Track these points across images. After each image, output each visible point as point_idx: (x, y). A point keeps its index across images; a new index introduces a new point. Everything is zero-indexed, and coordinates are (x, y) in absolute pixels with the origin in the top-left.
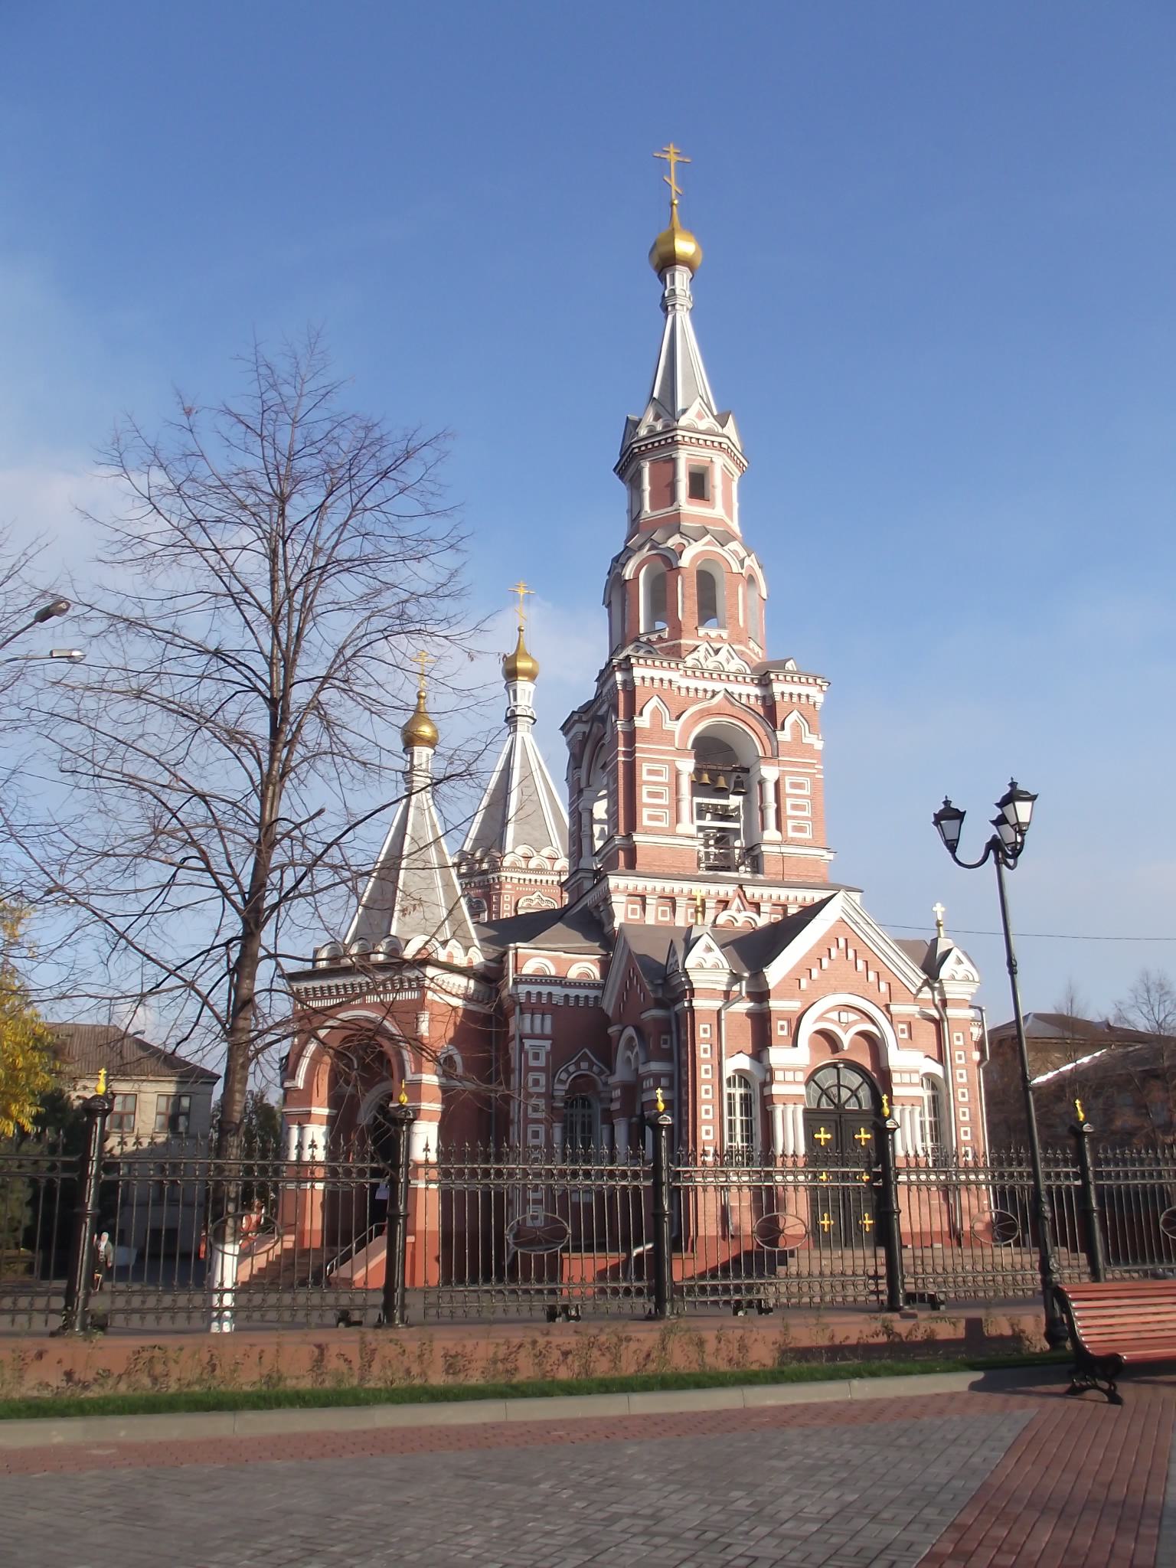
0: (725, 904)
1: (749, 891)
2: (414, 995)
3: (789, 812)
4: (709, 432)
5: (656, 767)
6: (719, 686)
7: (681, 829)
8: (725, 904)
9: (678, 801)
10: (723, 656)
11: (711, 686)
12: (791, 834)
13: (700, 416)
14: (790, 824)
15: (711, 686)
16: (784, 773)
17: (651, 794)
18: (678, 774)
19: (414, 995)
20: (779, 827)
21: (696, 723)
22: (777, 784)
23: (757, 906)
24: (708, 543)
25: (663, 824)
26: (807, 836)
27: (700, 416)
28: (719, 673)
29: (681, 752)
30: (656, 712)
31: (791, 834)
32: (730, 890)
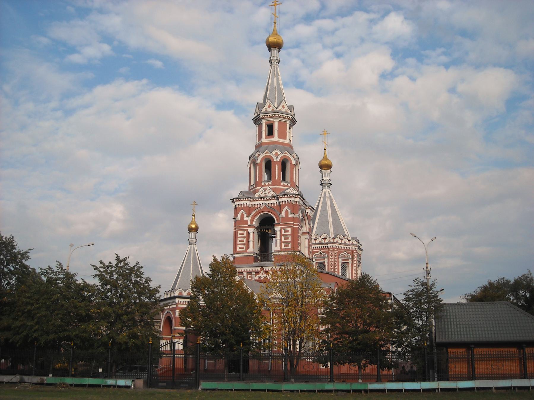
0: (257, 273)
1: (265, 268)
2: (175, 306)
3: (283, 240)
4: (273, 111)
5: (242, 232)
6: (263, 202)
7: (249, 250)
8: (257, 273)
9: (249, 242)
10: (267, 192)
11: (261, 202)
12: (283, 247)
13: (269, 106)
14: (283, 245)
15: (261, 202)
16: (282, 228)
17: (240, 241)
18: (249, 233)
19: (175, 306)
20: (281, 246)
21: (256, 216)
22: (281, 231)
23: (266, 272)
24: (267, 153)
25: (244, 250)
26: (290, 247)
27: (269, 106)
28: (266, 198)
29: (250, 226)
30: (242, 215)
31: (283, 247)
32: (259, 268)
